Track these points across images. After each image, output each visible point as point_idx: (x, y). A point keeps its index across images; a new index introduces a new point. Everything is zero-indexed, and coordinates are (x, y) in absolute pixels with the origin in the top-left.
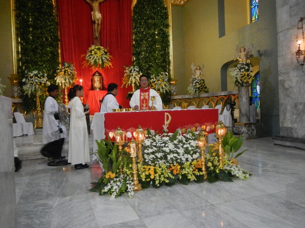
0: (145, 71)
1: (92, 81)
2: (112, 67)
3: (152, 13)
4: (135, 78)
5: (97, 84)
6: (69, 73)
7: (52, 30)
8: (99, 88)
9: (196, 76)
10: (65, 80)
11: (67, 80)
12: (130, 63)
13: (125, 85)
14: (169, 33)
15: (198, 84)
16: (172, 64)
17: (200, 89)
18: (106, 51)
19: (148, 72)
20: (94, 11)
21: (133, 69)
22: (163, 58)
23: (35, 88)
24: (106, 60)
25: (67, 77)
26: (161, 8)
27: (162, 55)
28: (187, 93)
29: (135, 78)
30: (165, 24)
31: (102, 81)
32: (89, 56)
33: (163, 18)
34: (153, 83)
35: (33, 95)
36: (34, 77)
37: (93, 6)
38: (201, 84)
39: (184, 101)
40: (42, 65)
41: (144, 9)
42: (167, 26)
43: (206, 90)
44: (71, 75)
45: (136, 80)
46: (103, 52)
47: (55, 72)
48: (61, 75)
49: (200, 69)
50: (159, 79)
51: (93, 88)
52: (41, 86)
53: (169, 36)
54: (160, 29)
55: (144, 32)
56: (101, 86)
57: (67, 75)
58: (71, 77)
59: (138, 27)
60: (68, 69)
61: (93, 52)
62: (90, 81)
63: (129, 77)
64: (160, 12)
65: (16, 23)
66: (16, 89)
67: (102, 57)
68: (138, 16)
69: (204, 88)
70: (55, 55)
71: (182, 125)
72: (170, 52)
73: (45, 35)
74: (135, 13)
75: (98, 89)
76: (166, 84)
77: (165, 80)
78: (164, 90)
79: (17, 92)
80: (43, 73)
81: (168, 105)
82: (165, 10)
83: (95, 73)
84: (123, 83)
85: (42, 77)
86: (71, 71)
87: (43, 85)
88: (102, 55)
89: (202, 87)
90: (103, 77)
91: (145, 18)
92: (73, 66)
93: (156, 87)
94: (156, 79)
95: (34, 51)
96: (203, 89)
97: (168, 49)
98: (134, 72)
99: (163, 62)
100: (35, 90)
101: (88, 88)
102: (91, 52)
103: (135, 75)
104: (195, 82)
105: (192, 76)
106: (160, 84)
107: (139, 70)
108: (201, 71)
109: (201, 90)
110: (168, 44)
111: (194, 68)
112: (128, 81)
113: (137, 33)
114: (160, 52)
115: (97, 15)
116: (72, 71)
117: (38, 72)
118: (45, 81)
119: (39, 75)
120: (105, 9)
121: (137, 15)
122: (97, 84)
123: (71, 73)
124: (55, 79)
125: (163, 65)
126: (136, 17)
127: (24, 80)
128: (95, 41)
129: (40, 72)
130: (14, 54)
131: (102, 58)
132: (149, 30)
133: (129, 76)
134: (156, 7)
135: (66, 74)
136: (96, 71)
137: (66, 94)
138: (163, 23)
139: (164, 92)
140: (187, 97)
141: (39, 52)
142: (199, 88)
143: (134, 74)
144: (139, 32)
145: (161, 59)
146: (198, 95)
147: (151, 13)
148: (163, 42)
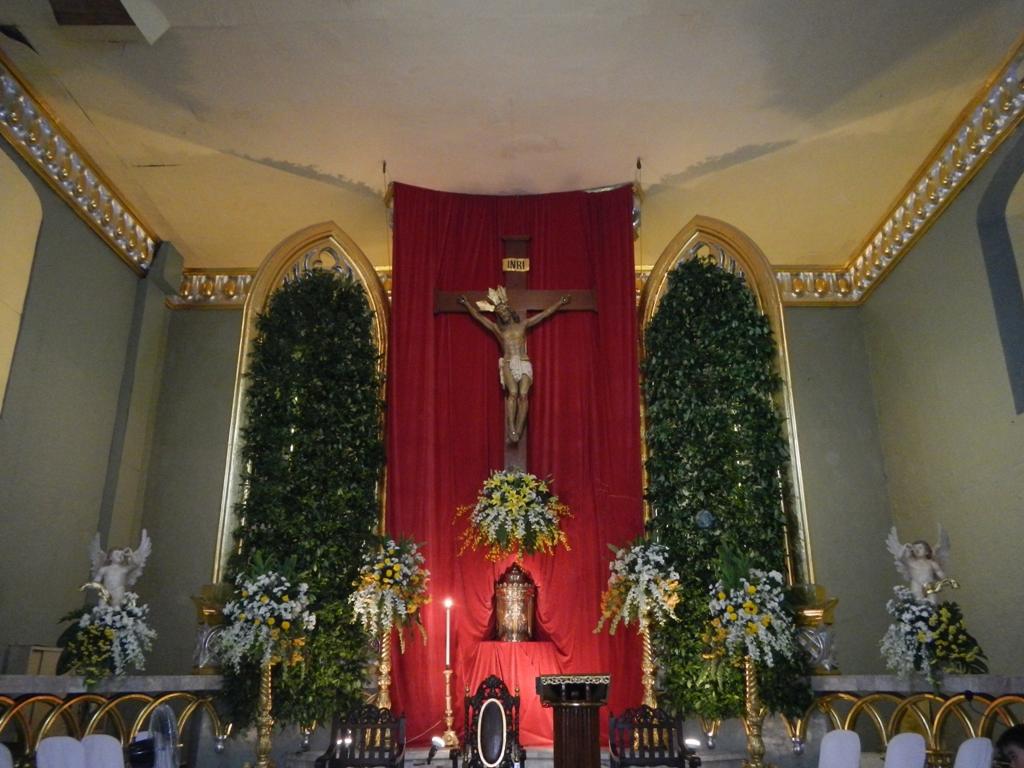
0: (694, 561)
1: (497, 602)
2: (568, 548)
3: (710, 344)
4: (648, 592)
5: (514, 615)
6: (398, 577)
7: (363, 428)
8: (518, 632)
9: (916, 589)
10: (381, 604)
11: (388, 607)
12: (632, 532)
13: (609, 621)
14: (784, 409)
15: (925, 628)
16: (804, 532)
17: (939, 653)
18: (543, 488)
19: (706, 566)
20: (506, 355)
21: (641, 555)
22: (762, 510)
23: (257, 636)
24: (542, 522)
25: (389, 593)
26: (741, 319)
27: (758, 498)
28: (878, 666)
29: (648, 592)
30: (763, 378)
31: (530, 603)
32: (485, 508)
33: (754, 357)
34: (718, 616)
36: (257, 598)
37: (503, 339)
38: (940, 623)
39: (872, 702)
40: (311, 552)
41: (683, 333)
42: (774, 384)
43: (969, 657)
44: (405, 583)
45: (655, 601)
46: (534, 495)
47: (354, 575)
48: (370, 583)
49: (929, 557)
50: (740, 600)
52: (278, 630)
53: (783, 419)
54: (746, 396)
55: (684, 411)
56: (526, 624)
57: (389, 583)
58: (402, 592)
59: (663, 397)
60: (397, 560)
61: (496, 495)
62: (489, 604)
63: (623, 589)
64: (744, 335)
67: (527, 511)
68: (663, 358)
69: (959, 646)
70: (365, 510)
72: (792, 485)
73: (335, 446)
74: (654, 347)
75: (514, 636)
76: (777, 624)
77: (769, 606)
78: (767, 649)
79: (210, 651)
81: (799, 717)
82: (761, 327)
83: (509, 571)
84: (601, 614)
85: (286, 598)
86: (406, 570)
87: (286, 625)
88: (528, 504)
89: (945, 644)
90: (536, 588)
91: (685, 362)
92: (418, 551)
93: (731, 638)
94: (731, 600)
95: (290, 503)
96: (953, 651)
97: (785, 471)
98: (646, 567)
99: (765, 527)
100: (253, 647)
101: (475, 632)
102: (489, 496)
103: (649, 581)
104: (907, 616)
105: (896, 588)
106: (746, 626)
107: (669, 561)
108: (935, 565)
109: (945, 659)
110: (781, 450)
111: (900, 554)
112: (619, 607)
113: (661, 416)
114: (749, 483)
115: (518, 368)
116: (409, 568)
117: (278, 579)
118: (298, 609)
119: (275, 590)
120: (548, 345)
121: (659, 354)
122: (514, 615)
123: (405, 576)
124: (350, 600)
125: (763, 537)
126: (654, 361)
127: (226, 611)
128: (508, 455)
129: (283, 579)
130: (227, 521)
131: (526, 517)
132: (704, 403)
133: (625, 586)
134: (724, 318)
135: (386, 580)
136: (509, 565)
137: (383, 655)
138: (753, 375)
139: (769, 661)
140: (882, 684)
141: (306, 504)
142: (931, 646)
143: (645, 577)
144: (669, 415)
145: (756, 514)
146: (929, 679)
147: (707, 342)
148: (758, 444)
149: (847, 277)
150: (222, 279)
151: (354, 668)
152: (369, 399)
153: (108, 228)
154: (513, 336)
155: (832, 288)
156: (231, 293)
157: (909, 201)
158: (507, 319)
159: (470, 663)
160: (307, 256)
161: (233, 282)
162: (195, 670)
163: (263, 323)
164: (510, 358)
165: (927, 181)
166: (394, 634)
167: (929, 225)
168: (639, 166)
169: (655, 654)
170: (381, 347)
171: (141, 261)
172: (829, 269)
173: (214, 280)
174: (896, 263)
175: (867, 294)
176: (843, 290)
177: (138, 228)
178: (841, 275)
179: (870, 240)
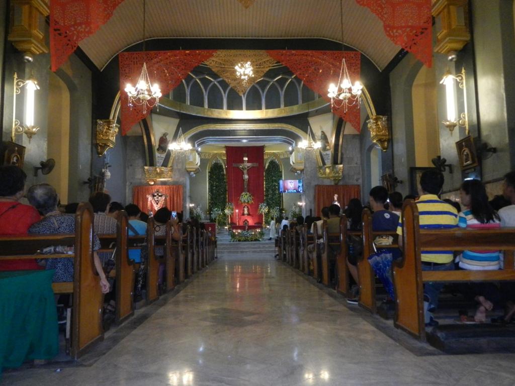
1: (244, 210)
5: (246, 212)
12: (263, 201)
35: (215, 219)
47: (224, 207)
51: (243, 214)
65: (209, 186)
66: (208, 216)
70: (225, 198)
71: (250, 229)
80: (219, 208)
95: (216, 198)
115: (246, 177)
122: (246, 212)
130: (208, 201)
133: (261, 208)
151: (225, 219)
152: (225, 182)
154: (245, 172)
159: (240, 218)
162: (207, 219)
163: (209, 172)
166: (231, 216)
169: (265, 217)
170: (225, 173)
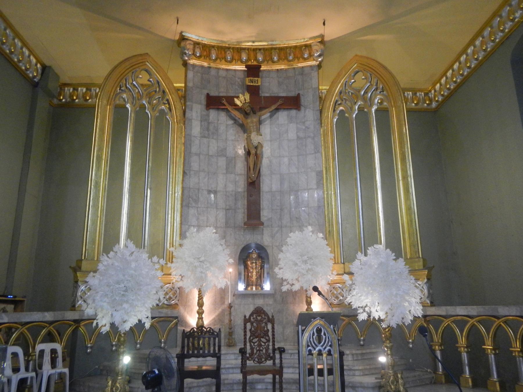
149: (430, 95)
150: (82, 90)
153: (13, 56)
155: (421, 101)
156: (88, 98)
157: (469, 51)
158: (249, 111)
160: (133, 73)
161: (88, 92)
164: (250, 133)
165: (481, 39)
167: (480, 64)
168: (324, 24)
171: (34, 77)
172: (420, 90)
173: (77, 90)
174: (459, 86)
175: (441, 105)
176: (427, 102)
177: (32, 57)
178: (426, 94)
179: (445, 74)
